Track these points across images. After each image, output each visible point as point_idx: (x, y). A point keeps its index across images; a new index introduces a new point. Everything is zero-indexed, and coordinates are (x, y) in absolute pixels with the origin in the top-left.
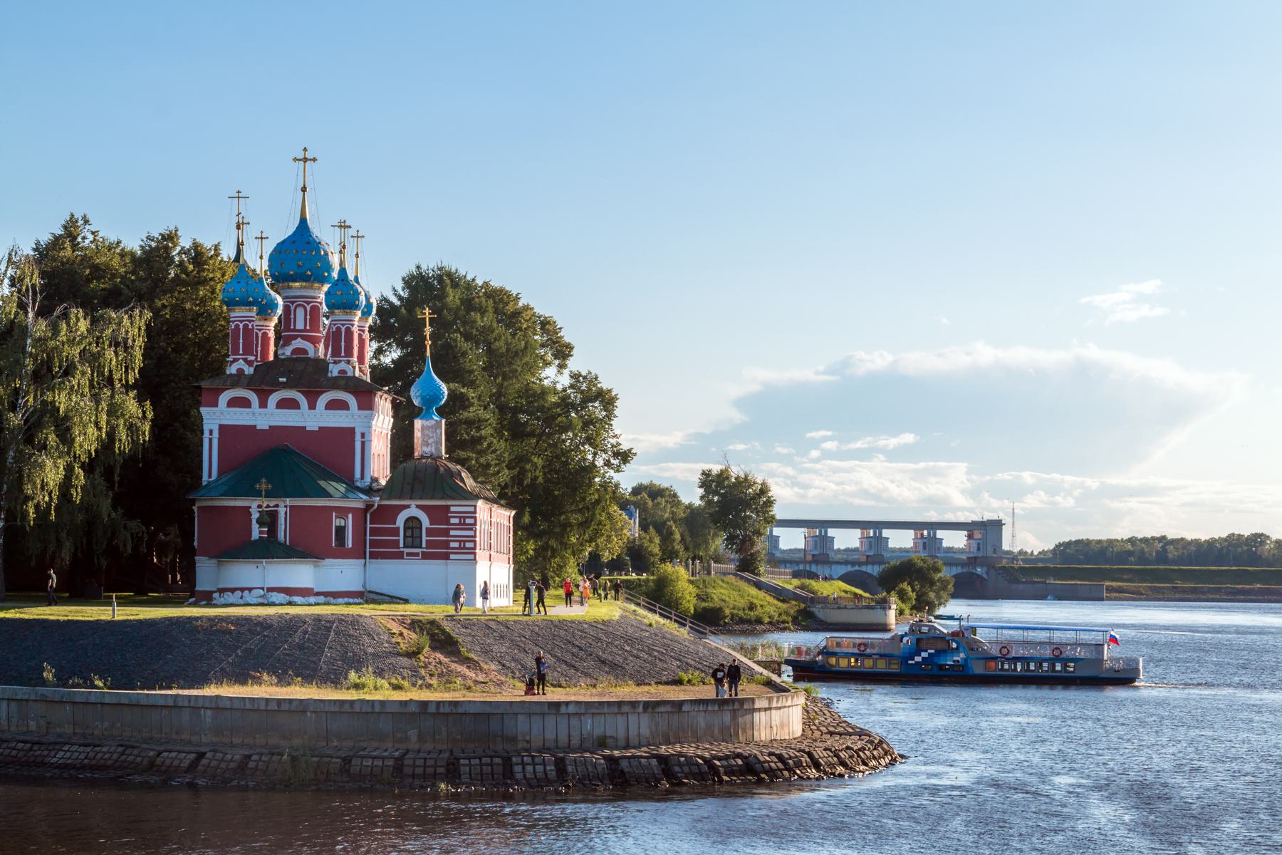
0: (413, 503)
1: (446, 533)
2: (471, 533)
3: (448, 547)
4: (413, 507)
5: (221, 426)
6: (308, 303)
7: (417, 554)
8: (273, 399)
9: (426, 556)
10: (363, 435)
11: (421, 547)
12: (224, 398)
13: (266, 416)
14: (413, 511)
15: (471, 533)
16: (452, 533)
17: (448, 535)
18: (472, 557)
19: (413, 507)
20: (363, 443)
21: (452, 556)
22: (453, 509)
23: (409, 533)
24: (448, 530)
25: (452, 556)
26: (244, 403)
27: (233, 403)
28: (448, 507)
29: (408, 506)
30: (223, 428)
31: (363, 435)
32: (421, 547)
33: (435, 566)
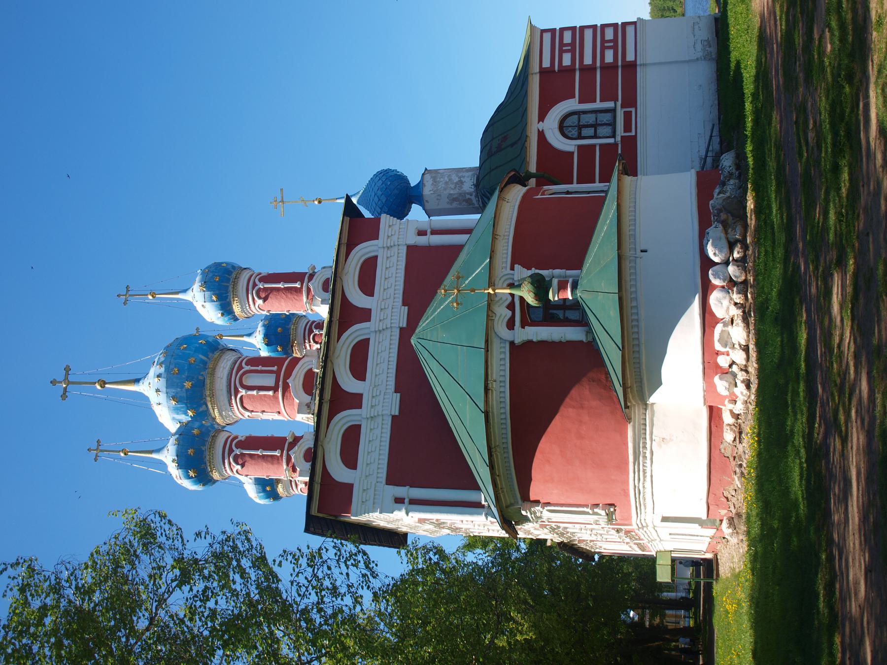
0: (534, 126)
1: (588, 71)
2: (588, 34)
3: (613, 67)
4: (541, 126)
5: (391, 480)
6: (240, 368)
7: (627, 117)
8: (349, 384)
9: (630, 100)
10: (422, 233)
11: (613, 111)
12: (340, 473)
13: (379, 400)
14: (550, 125)
15: (588, 34)
16: (588, 61)
17: (592, 69)
18: (630, 30)
19: (541, 126)
20: (434, 232)
21: (630, 57)
22: (546, 64)
23: (590, 131)
24: (585, 69)
25: (630, 57)
26: (352, 436)
27: (350, 458)
28: (543, 72)
29: (541, 135)
30: (391, 480)
31: (422, 233)
32: (613, 111)
33: (648, 84)
